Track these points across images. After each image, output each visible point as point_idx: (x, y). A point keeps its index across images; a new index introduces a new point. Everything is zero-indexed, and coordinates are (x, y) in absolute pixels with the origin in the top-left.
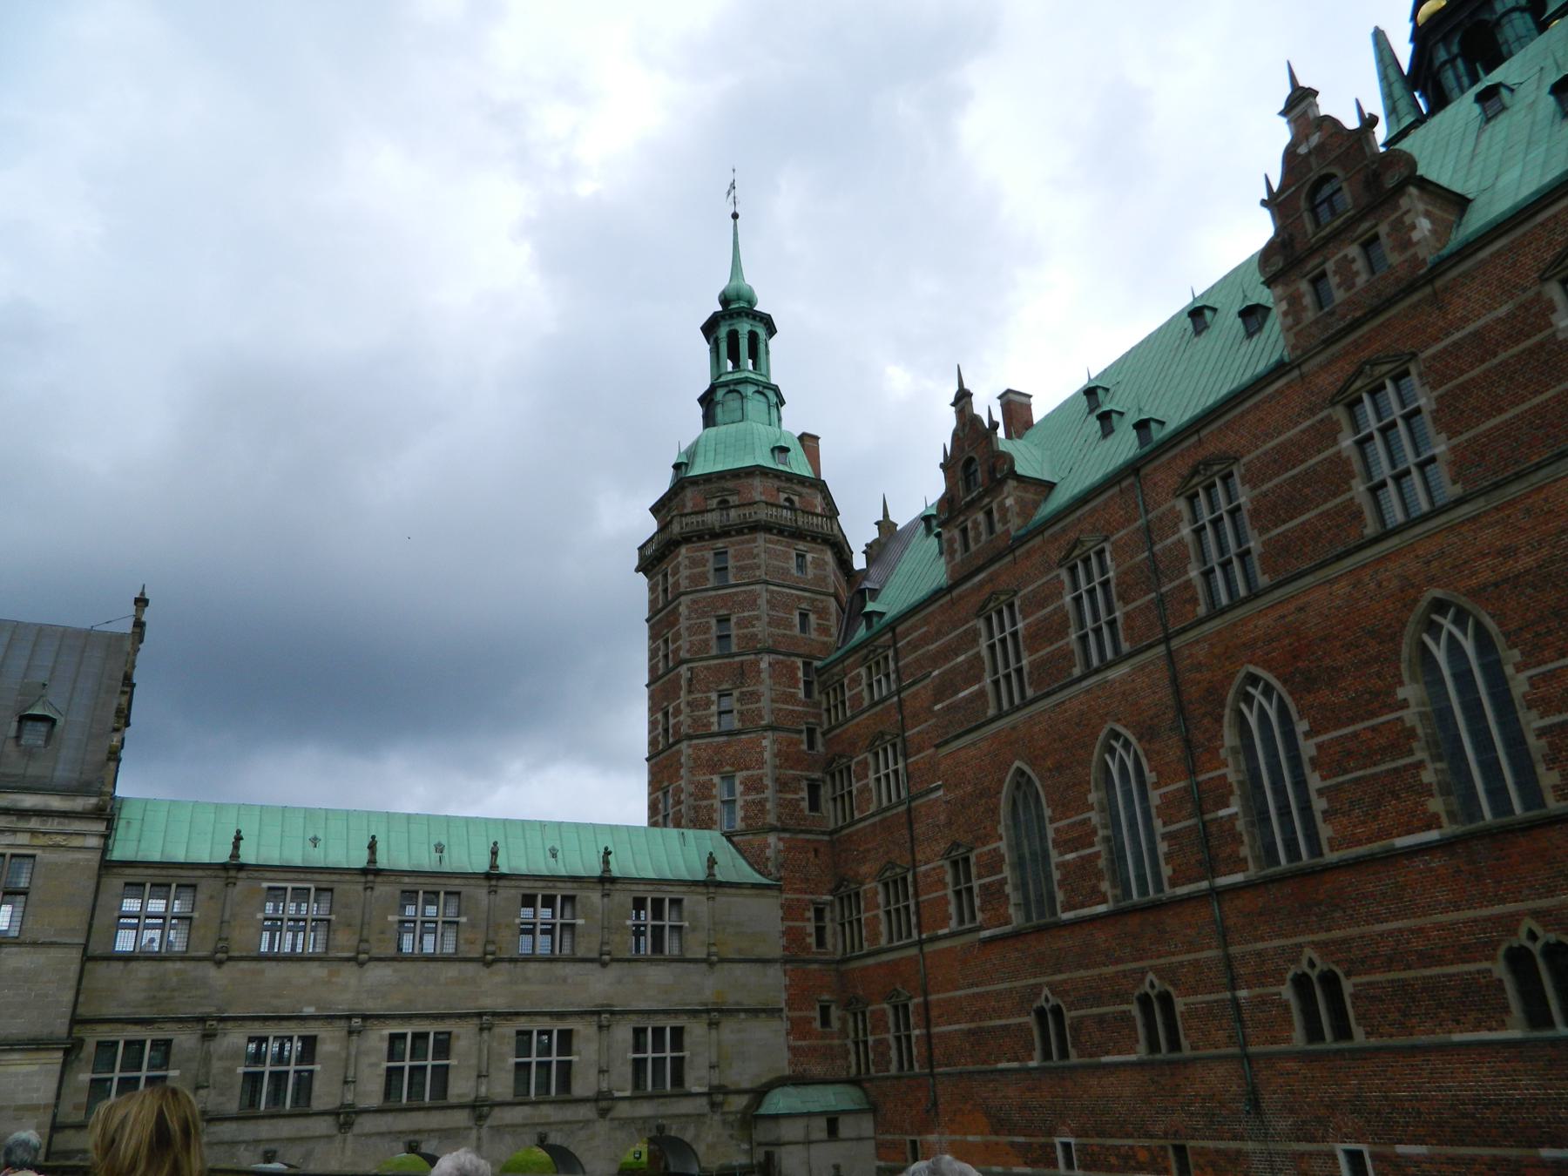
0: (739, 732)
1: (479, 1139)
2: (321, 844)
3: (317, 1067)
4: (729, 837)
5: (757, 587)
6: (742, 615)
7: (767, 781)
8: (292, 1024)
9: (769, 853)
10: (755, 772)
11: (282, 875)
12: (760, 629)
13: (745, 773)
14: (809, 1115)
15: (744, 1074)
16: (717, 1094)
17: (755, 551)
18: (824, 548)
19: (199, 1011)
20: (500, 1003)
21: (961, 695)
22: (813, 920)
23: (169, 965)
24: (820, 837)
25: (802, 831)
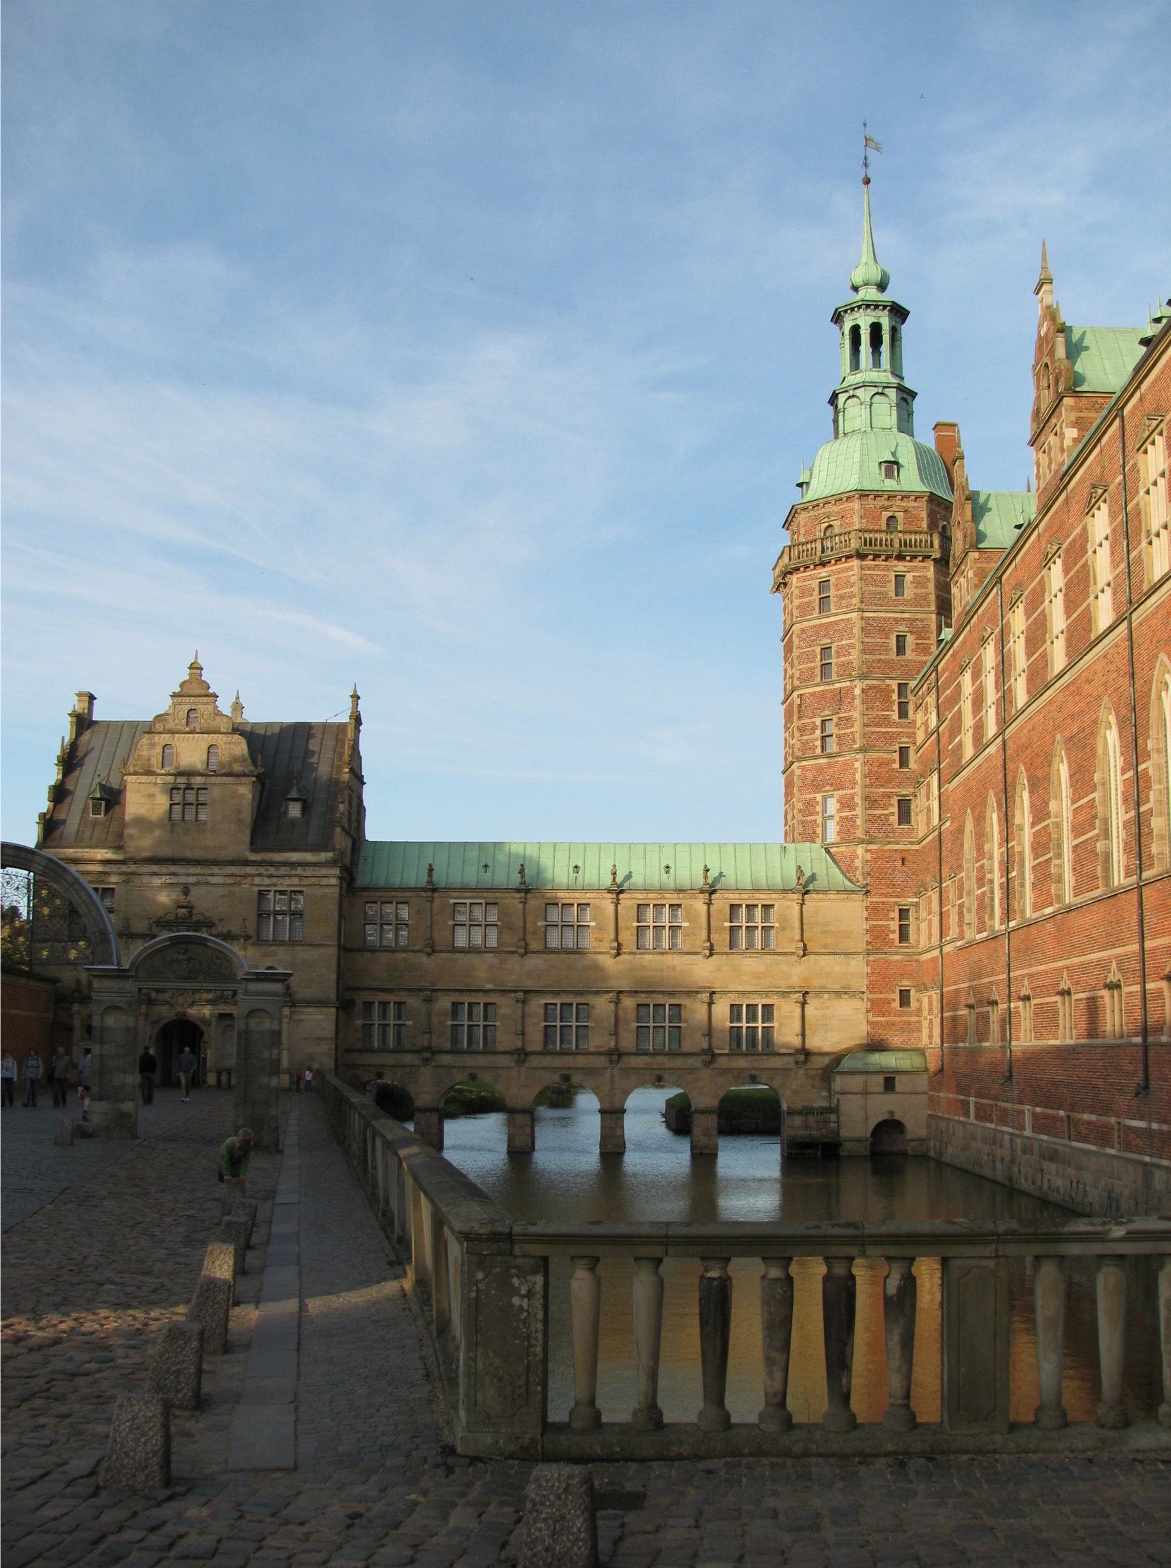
1: (612, 1076)
2: (490, 870)
7: (858, 800)
8: (479, 994)
9: (858, 863)
13: (842, 792)
25: (889, 843)
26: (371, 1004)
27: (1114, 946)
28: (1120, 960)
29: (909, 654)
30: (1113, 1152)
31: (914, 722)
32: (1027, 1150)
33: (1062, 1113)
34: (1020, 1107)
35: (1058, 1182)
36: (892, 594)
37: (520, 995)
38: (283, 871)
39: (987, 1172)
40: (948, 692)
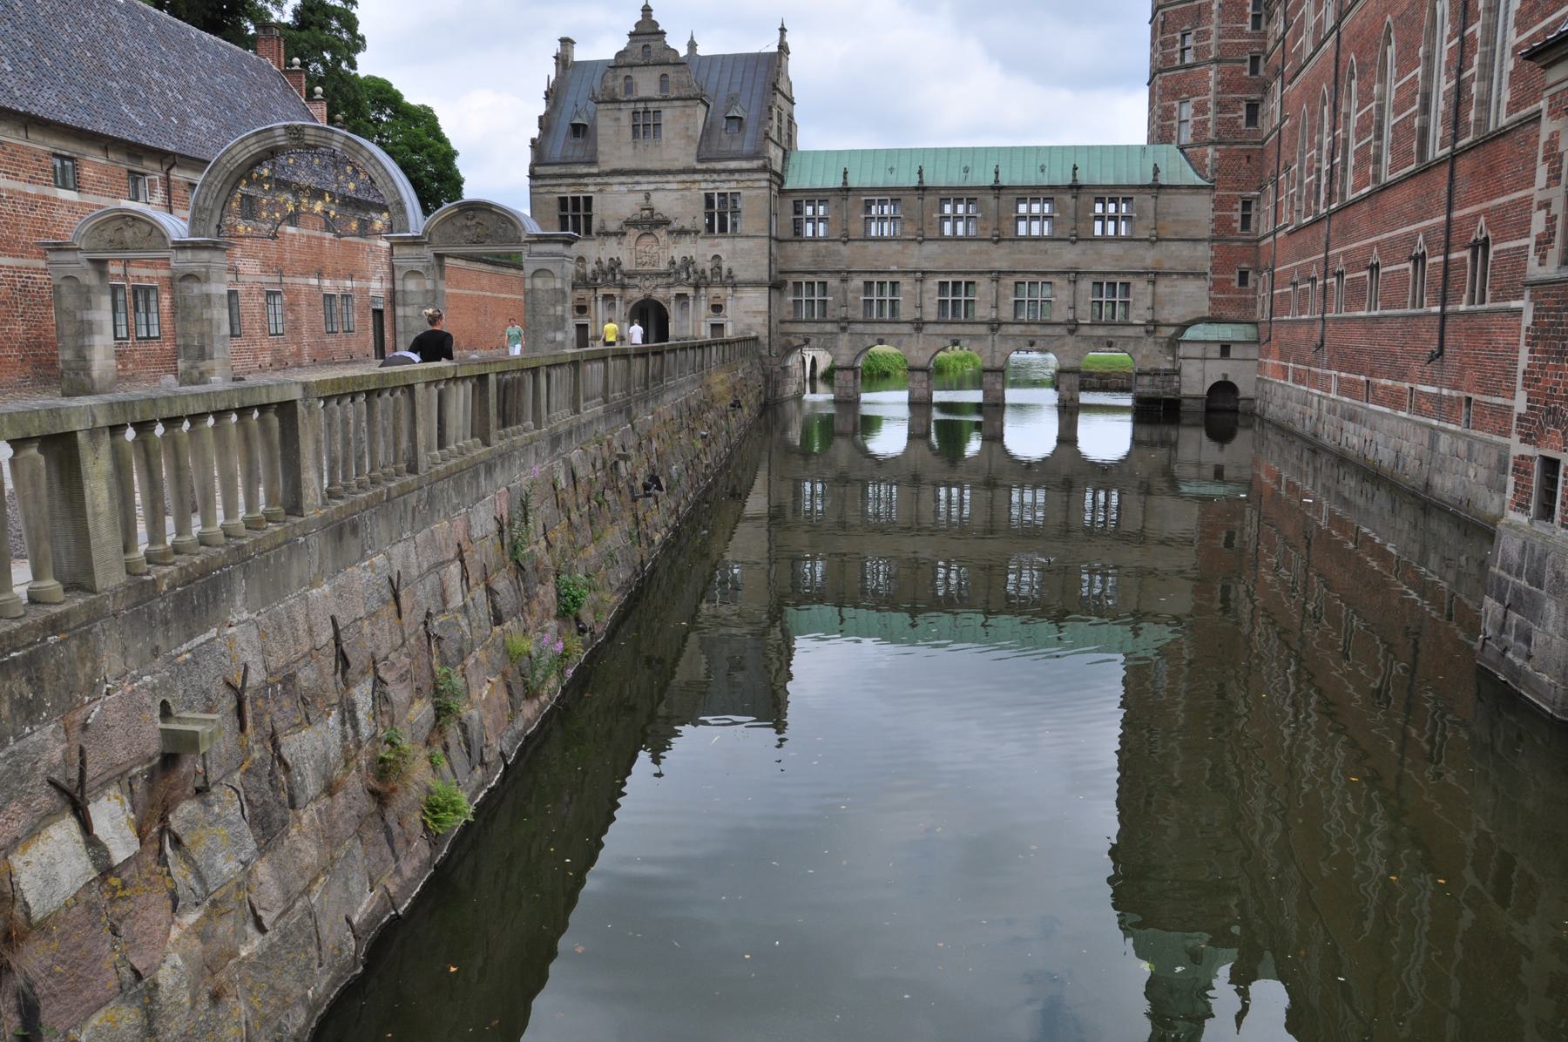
4: (1182, 149)
7: (1210, 105)
8: (886, 275)
9: (1208, 161)
13: (1196, 99)
16: (1153, 325)
19: (838, 268)
20: (1003, 265)
23: (821, 244)
25: (1236, 143)
26: (813, 283)
27: (1422, 219)
28: (1427, 232)
30: (1404, 414)
31: (1265, 33)
32: (1332, 411)
33: (1363, 378)
34: (1328, 372)
35: (1355, 441)
37: (919, 275)
38: (723, 177)
39: (1298, 428)
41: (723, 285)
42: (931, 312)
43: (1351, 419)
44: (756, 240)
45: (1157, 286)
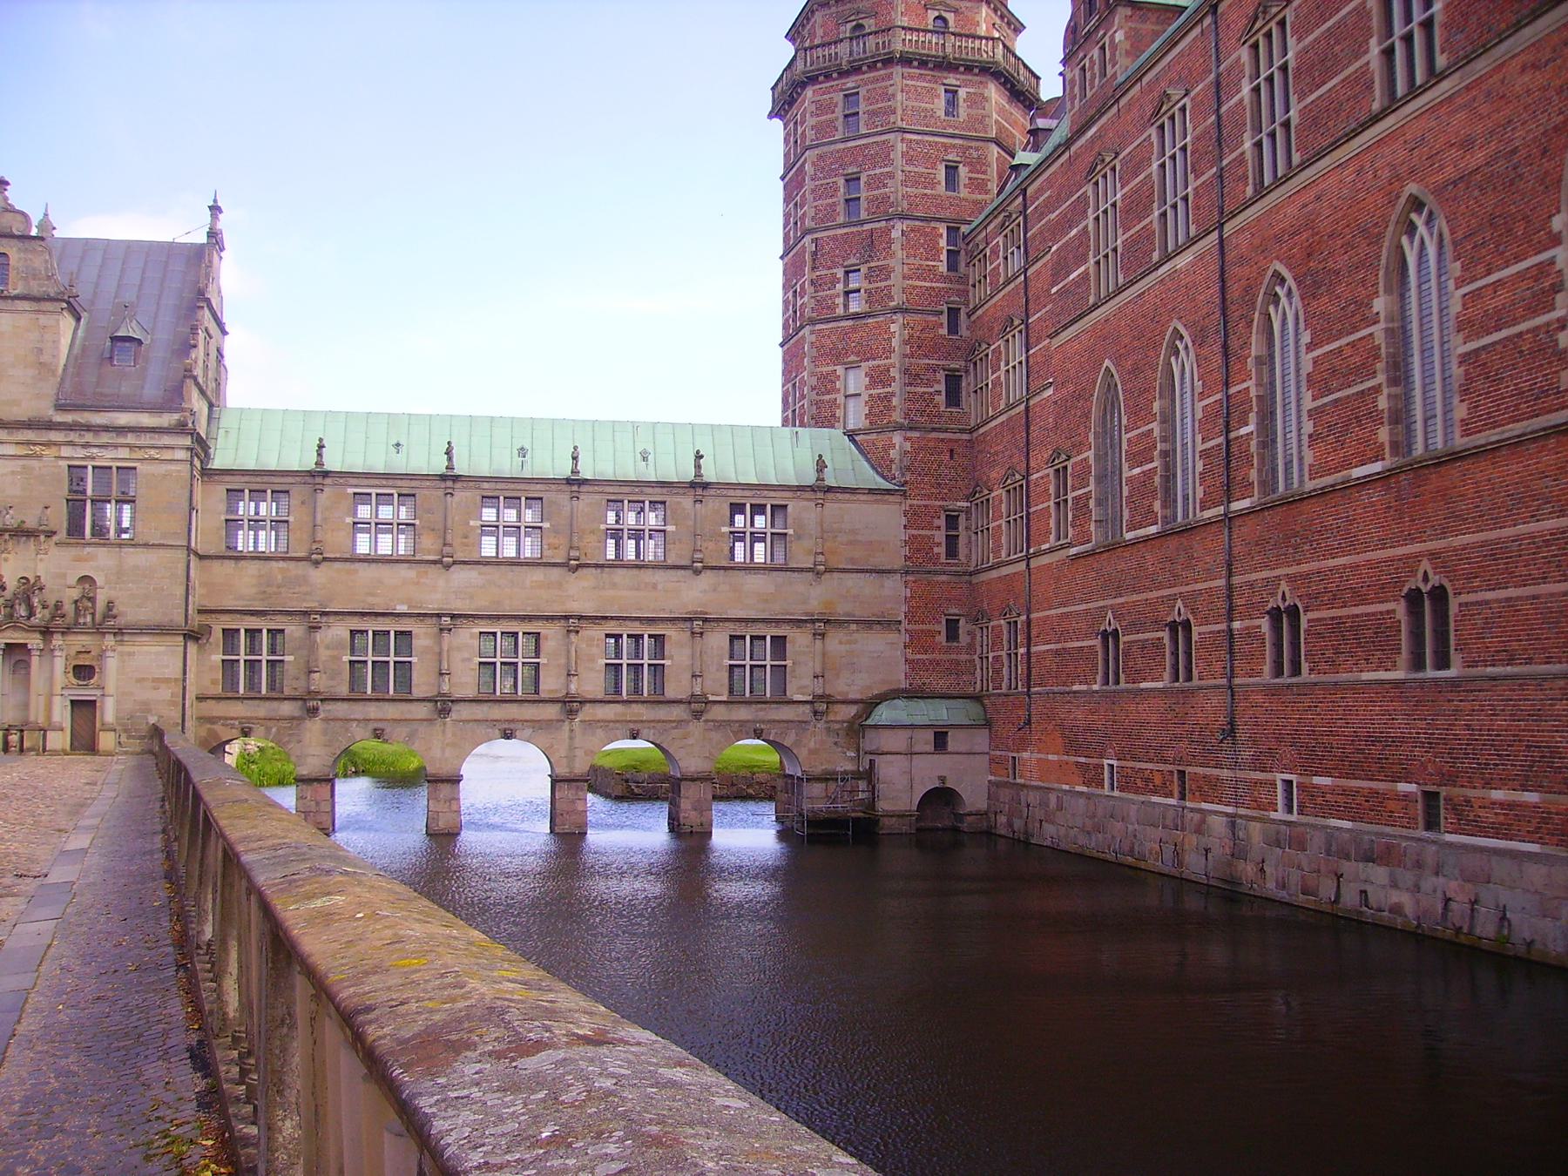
0: (867, 315)
2: (404, 449)
3: (414, 659)
4: (851, 435)
5: (891, 136)
6: (872, 173)
7: (894, 373)
8: (387, 620)
10: (883, 362)
11: (366, 482)
12: (896, 190)
13: (871, 363)
14: (912, 727)
15: (853, 685)
16: (822, 703)
17: (891, 91)
18: (984, 79)
19: (303, 606)
20: (588, 608)
21: (1071, 277)
22: (943, 528)
23: (274, 564)
24: (958, 436)
25: (934, 430)
29: (964, 193)
31: (967, 276)
36: (941, 113)
38: (105, 438)
40: (1052, 216)
41: (99, 630)
42: (592, 682)
43: (1368, 858)
44: (162, 552)
45: (827, 640)
